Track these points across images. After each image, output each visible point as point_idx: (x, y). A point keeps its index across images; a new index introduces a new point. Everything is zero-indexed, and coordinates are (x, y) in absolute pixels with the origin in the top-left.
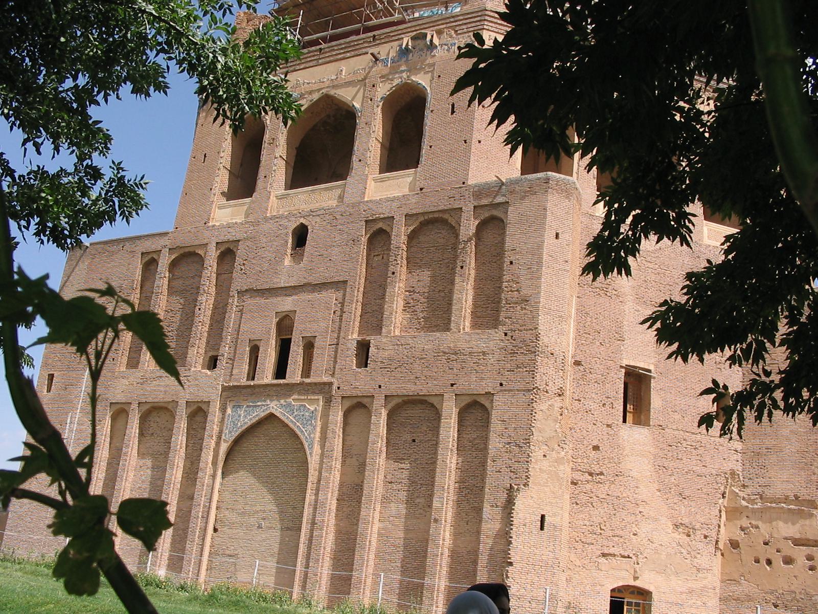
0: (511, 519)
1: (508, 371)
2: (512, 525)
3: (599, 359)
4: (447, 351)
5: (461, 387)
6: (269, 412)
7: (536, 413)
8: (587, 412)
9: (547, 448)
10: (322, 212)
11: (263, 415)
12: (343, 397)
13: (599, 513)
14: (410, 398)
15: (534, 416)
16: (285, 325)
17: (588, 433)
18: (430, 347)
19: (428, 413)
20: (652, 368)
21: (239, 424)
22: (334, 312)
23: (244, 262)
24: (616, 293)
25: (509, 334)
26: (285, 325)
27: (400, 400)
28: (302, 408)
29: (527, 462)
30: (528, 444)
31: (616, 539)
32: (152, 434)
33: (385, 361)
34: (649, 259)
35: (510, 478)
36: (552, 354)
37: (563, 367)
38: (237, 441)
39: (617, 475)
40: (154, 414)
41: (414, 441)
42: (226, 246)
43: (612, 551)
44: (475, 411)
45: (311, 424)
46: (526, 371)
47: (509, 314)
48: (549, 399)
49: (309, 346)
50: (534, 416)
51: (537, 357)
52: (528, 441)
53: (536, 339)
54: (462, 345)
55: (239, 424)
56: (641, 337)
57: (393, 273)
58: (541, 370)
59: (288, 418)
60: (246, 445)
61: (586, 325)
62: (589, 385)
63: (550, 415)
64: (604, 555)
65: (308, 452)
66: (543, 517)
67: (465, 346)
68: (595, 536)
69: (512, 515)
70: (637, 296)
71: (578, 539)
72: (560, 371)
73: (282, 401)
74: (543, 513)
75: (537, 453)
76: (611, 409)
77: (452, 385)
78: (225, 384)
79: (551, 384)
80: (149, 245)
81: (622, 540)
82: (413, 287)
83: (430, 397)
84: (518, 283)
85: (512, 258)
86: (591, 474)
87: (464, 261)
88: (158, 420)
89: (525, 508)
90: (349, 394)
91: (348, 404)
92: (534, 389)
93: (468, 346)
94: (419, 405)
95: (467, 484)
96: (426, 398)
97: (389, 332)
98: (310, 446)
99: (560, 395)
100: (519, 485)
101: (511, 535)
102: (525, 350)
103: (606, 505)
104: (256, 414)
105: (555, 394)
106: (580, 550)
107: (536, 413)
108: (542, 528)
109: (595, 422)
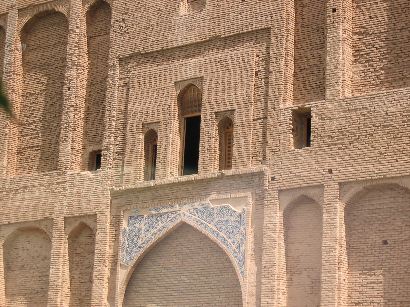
6: (177, 221)
11: (171, 225)
12: (280, 191)
14: (374, 183)
16: (189, 99)
18: (395, 109)
19: (403, 202)
21: (140, 242)
22: (257, 74)
23: (124, 17)
26: (189, 99)
27: (360, 188)
28: (225, 212)
32: (23, 266)
33: (334, 135)
38: (139, 266)
41: (385, 242)
45: (239, 233)
49: (226, 125)
55: (140, 242)
57: (334, 10)
59: (207, 227)
60: (152, 270)
65: (239, 271)
73: (196, 205)
78: (115, 188)
82: (364, 27)
83: (403, 180)
88: (29, 246)
90: (288, 185)
91: (287, 199)
94: (389, 192)
96: (397, 182)
97: (336, 94)
104: (161, 225)
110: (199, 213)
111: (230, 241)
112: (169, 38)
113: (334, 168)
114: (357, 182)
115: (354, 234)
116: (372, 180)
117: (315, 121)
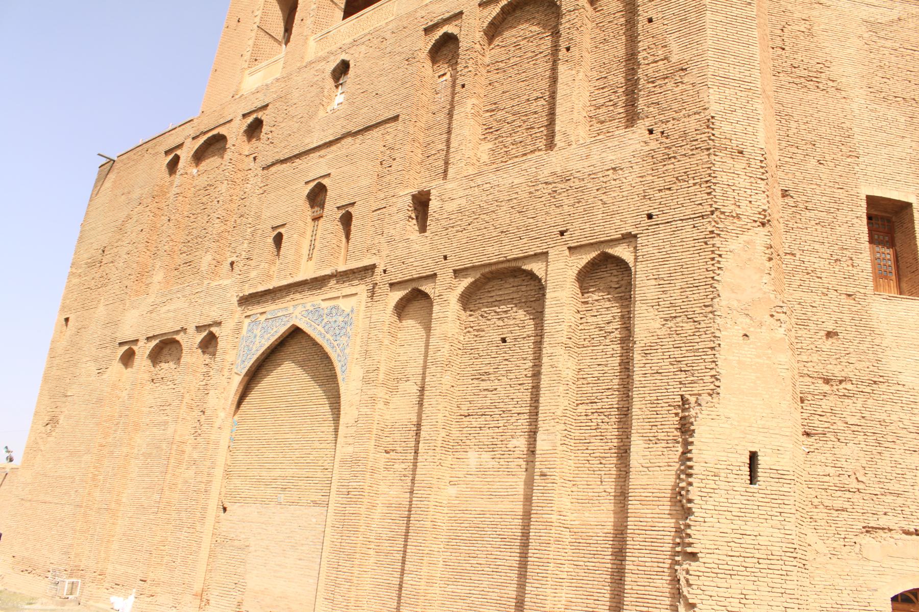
0: (689, 463)
1: (660, 191)
2: (690, 475)
3: (820, 186)
4: (550, 180)
5: (577, 233)
7: (720, 256)
8: (808, 273)
9: (748, 320)
10: (367, 38)
13: (852, 453)
14: (494, 268)
15: (719, 262)
17: (814, 310)
18: (522, 180)
19: (527, 291)
20: (910, 199)
21: (254, 349)
23: (273, 129)
24: (834, 84)
25: (657, 131)
28: (334, 311)
29: (713, 348)
30: (711, 315)
31: (889, 499)
34: (882, 34)
35: (681, 383)
36: (741, 152)
37: (763, 173)
39: (875, 382)
40: (165, 351)
41: (504, 340)
42: (254, 116)
43: (883, 522)
44: (606, 271)
46: (695, 184)
47: (654, 99)
48: (745, 230)
49: (347, 220)
50: (719, 262)
51: (713, 157)
52: (710, 309)
53: (708, 127)
54: (576, 165)
56: (886, 151)
57: (463, 86)
58: (723, 178)
61: (790, 133)
62: (806, 228)
63: (750, 260)
64: (869, 530)
66: (753, 457)
67: (579, 166)
68: (848, 495)
69: (689, 455)
70: (871, 90)
71: (816, 501)
72: (759, 181)
74: (753, 450)
75: (729, 334)
76: (850, 268)
77: (562, 233)
79: (744, 203)
80: (171, 142)
81: (900, 501)
82: (495, 104)
84: (666, 46)
85: (650, 14)
86: (827, 381)
87: (572, 39)
89: (718, 442)
91: (398, 295)
92: (712, 213)
93: (586, 164)
94: (512, 280)
95: (599, 405)
96: (519, 264)
98: (344, 368)
99: (763, 224)
100: (700, 395)
101: (690, 497)
102: (688, 152)
103: (861, 438)
105: (755, 221)
106: (823, 523)
107: (720, 256)
108: (753, 479)
109: (825, 291)
110: (310, 315)
111: (335, 344)
112: (306, 142)
113: (448, 254)
114: (474, 268)
115: (469, 332)
116: (490, 264)
117: (434, 205)
